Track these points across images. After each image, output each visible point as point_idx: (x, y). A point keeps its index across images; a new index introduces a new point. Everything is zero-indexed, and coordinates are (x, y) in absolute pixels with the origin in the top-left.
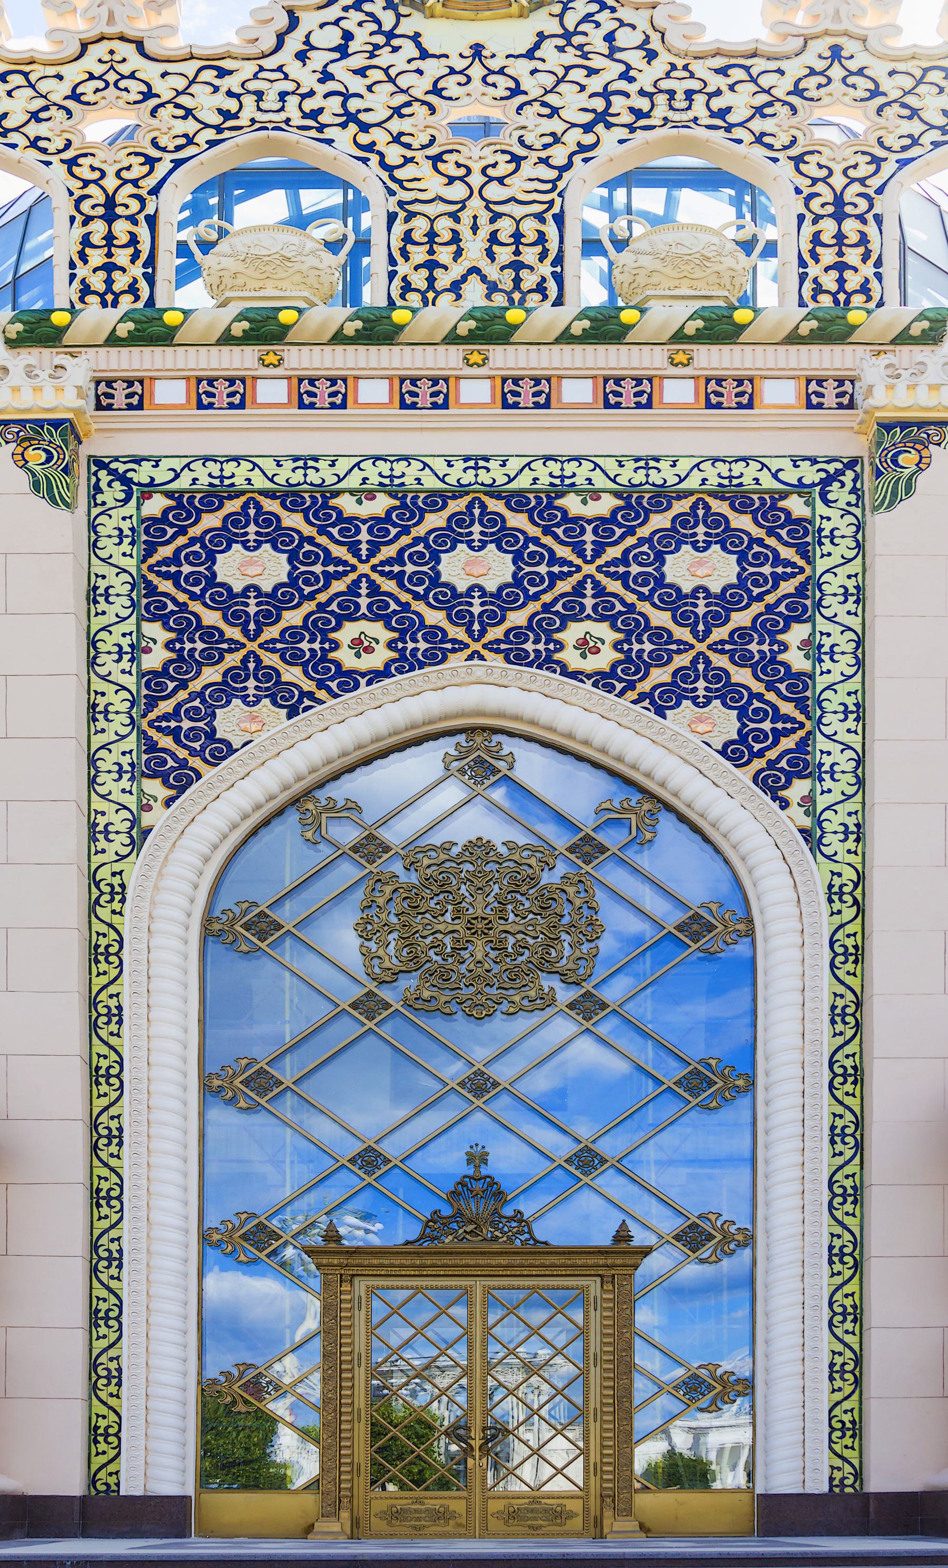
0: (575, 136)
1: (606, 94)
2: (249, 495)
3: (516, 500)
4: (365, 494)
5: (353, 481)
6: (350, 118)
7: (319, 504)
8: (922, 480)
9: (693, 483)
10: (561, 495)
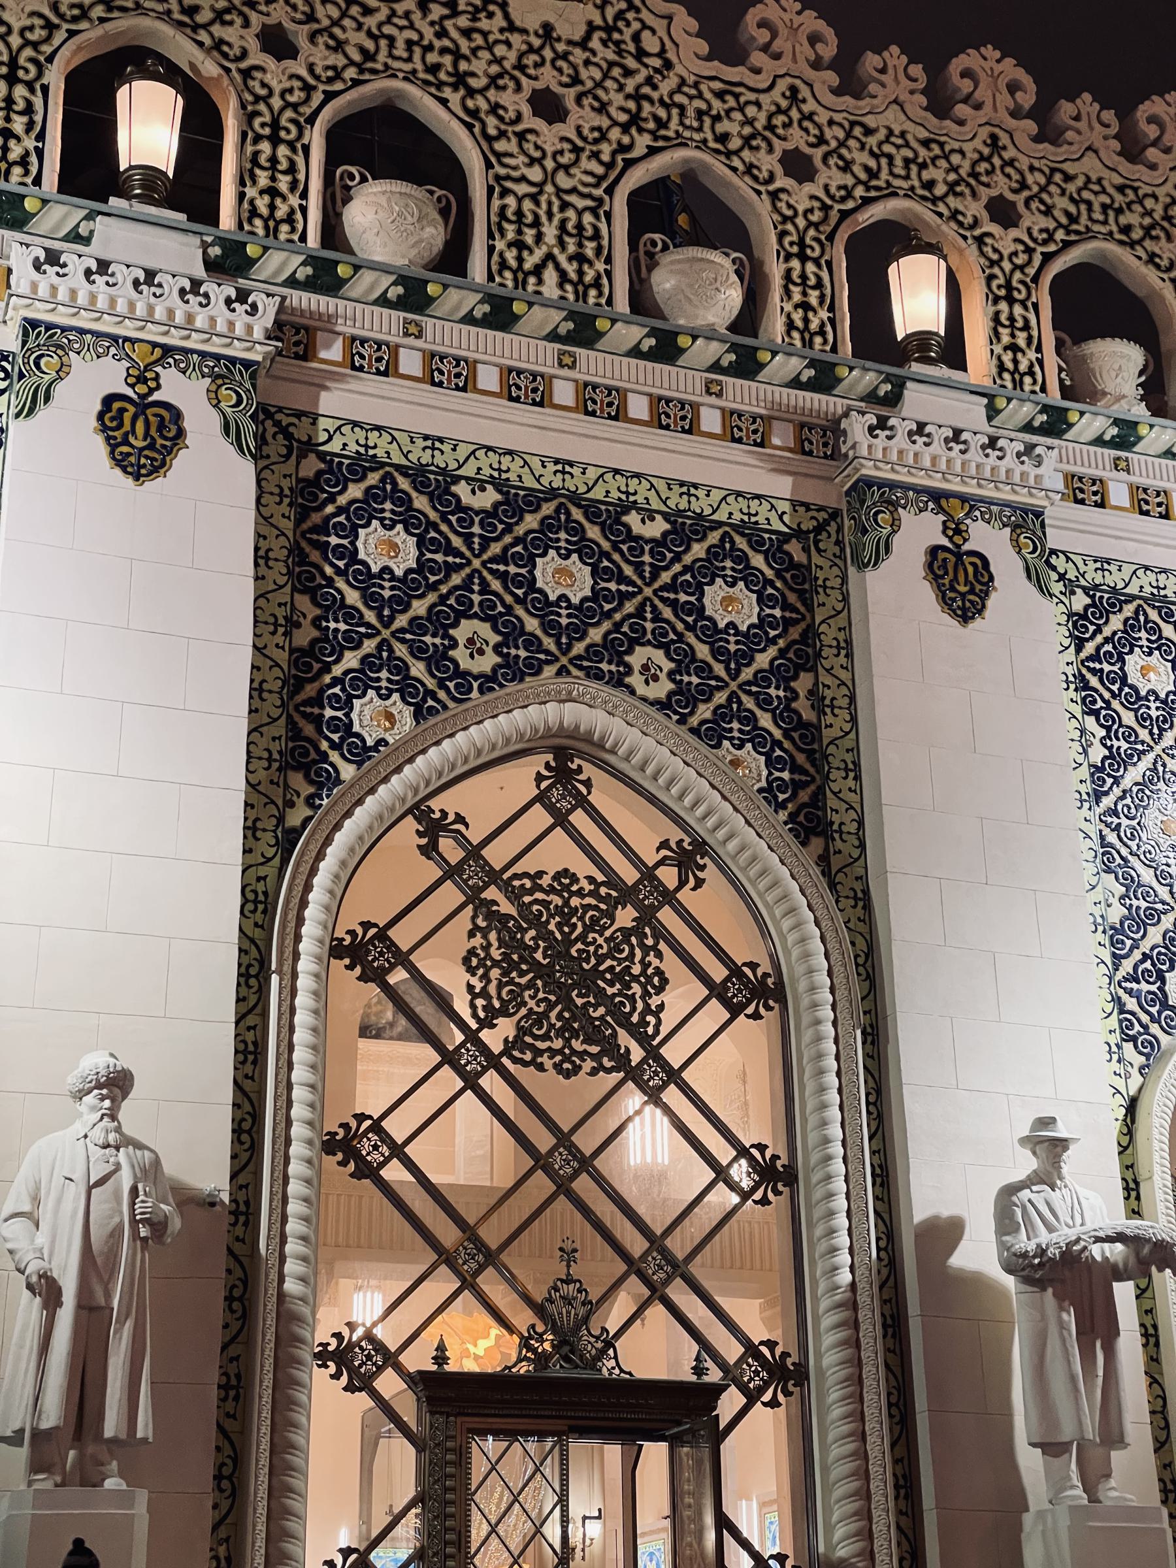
0: (615, 134)
1: (637, 97)
2: (387, 469)
3: (592, 510)
4: (477, 484)
5: (469, 470)
6: (460, 80)
7: (438, 483)
8: (896, 540)
9: (721, 516)
10: (626, 510)
